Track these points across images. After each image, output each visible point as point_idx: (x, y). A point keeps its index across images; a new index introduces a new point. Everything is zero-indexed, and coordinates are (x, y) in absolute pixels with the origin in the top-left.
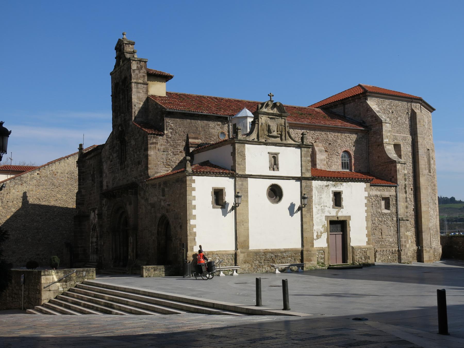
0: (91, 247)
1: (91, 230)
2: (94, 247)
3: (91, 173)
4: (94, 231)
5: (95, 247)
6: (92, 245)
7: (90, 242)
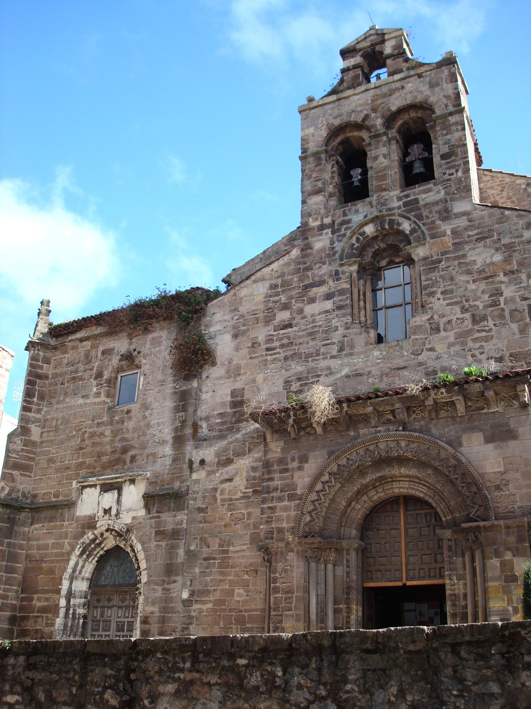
0: (62, 612)
1: (77, 552)
2: (74, 610)
3: (99, 375)
4: (88, 556)
5: (81, 611)
6: (68, 602)
7: (64, 592)
